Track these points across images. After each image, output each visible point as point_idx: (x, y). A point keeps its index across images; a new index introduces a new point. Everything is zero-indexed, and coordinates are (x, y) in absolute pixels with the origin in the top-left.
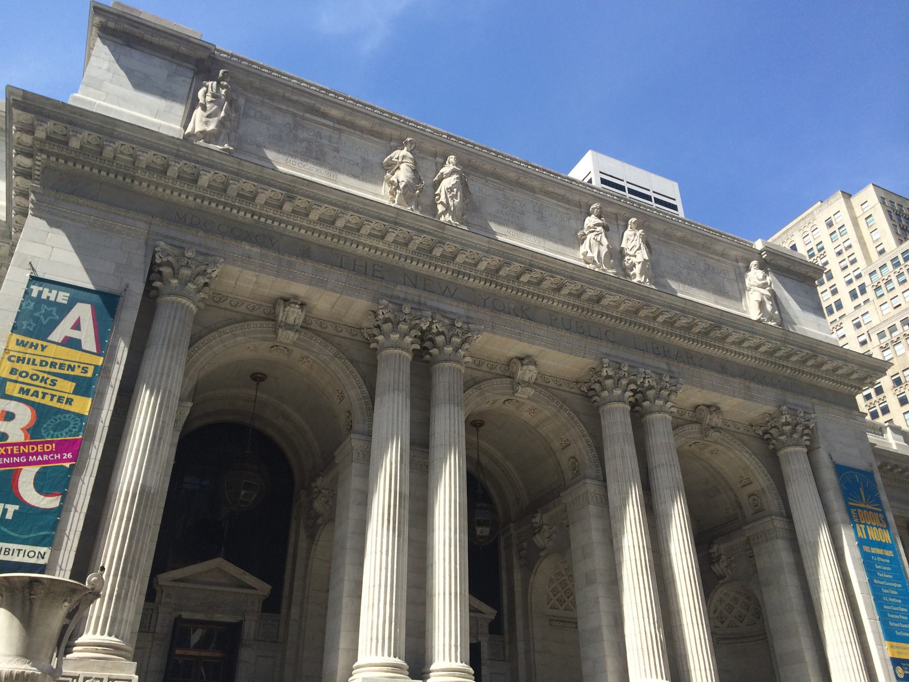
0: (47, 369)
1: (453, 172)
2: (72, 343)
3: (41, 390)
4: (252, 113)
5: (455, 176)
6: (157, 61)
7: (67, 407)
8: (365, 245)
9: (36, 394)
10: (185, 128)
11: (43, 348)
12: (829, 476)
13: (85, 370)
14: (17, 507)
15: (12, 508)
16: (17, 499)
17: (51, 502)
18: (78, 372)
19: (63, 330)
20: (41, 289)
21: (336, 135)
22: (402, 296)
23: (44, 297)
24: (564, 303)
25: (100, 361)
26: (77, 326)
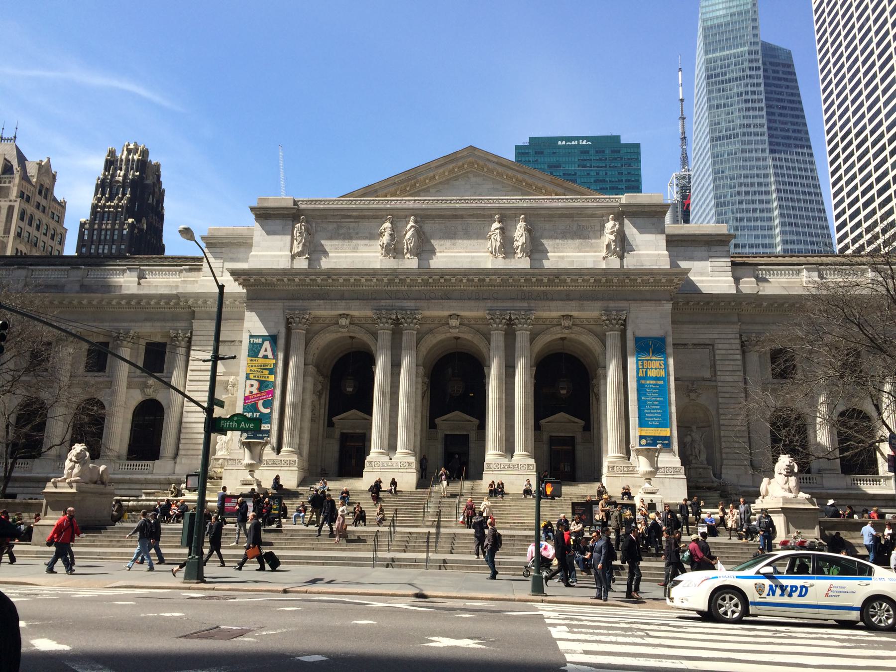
1: (412, 227)
2: (265, 357)
4: (319, 229)
5: (413, 229)
6: (278, 222)
7: (267, 379)
8: (365, 286)
10: (291, 252)
12: (631, 344)
15: (258, 414)
16: (257, 410)
17: (268, 411)
18: (269, 367)
21: (356, 225)
22: (384, 304)
24: (466, 286)
25: (274, 361)
26: (266, 350)
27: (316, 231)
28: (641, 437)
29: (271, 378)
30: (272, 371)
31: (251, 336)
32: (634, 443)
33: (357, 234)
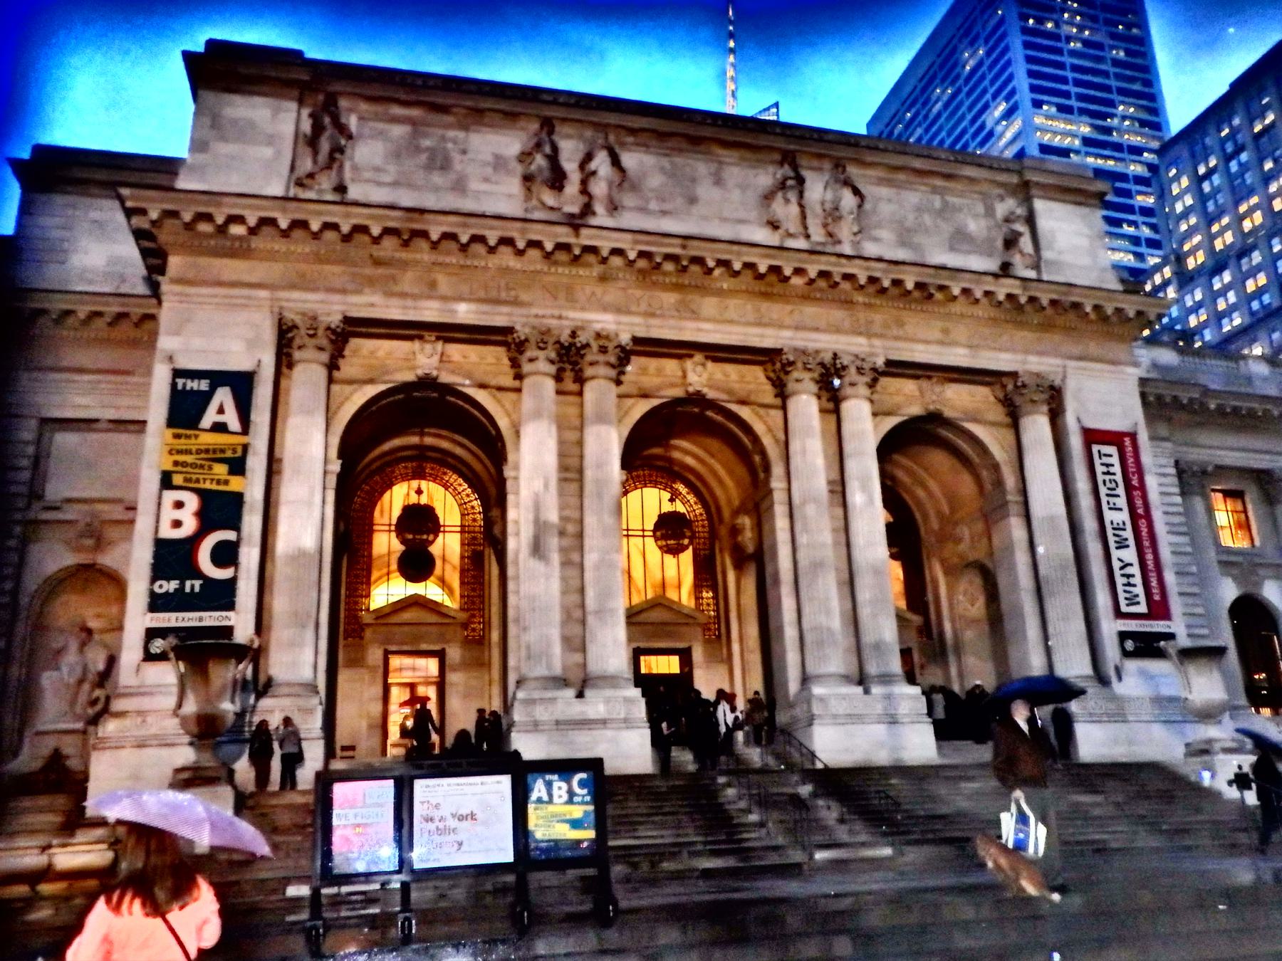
0: (203, 456)
2: (220, 428)
3: (201, 477)
4: (366, 131)
9: (198, 481)
11: (196, 437)
12: (1075, 442)
13: (234, 451)
14: (201, 582)
15: (197, 584)
16: (198, 574)
18: (229, 454)
19: (209, 418)
20: (184, 380)
21: (460, 135)
23: (188, 388)
25: (243, 439)
26: (221, 411)
27: (361, 136)
28: (1123, 636)
29: (235, 484)
30: (238, 466)
31: (178, 373)
32: (1111, 651)
33: (464, 152)
